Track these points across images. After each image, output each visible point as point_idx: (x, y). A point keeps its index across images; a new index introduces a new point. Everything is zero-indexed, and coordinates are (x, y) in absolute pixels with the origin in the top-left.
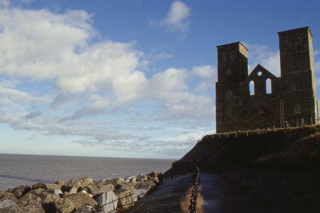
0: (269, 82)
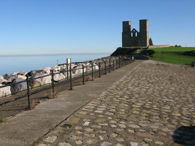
0: (136, 33)
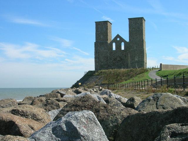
0: (123, 44)
